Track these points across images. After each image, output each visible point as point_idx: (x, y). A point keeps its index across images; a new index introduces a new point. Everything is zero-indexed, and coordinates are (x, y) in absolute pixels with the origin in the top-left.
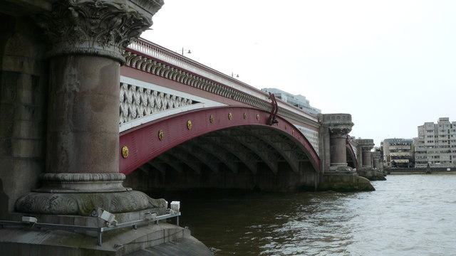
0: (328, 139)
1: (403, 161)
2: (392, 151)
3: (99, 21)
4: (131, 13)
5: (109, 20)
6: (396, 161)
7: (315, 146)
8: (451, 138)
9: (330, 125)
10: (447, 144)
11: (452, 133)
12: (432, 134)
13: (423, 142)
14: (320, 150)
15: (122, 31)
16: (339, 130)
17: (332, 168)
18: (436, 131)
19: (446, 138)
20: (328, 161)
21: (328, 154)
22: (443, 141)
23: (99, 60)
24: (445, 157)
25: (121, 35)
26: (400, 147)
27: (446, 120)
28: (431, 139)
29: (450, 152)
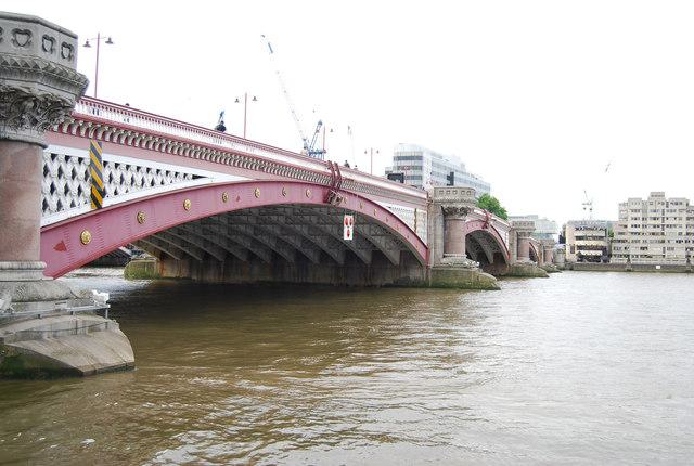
0: (440, 221)
1: (593, 253)
2: (579, 238)
3: (8, 105)
4: (44, 96)
5: (20, 103)
6: (583, 252)
7: (422, 232)
8: (666, 222)
9: (443, 202)
10: (659, 230)
11: (667, 215)
12: (639, 215)
13: (626, 227)
14: (429, 236)
15: (38, 114)
16: (455, 210)
17: (444, 260)
18: (645, 211)
19: (659, 222)
20: (440, 251)
21: (440, 241)
22: (655, 227)
23: (13, 145)
25: (37, 117)
26: (589, 233)
27: (661, 195)
28: (635, 222)
29: (663, 241)
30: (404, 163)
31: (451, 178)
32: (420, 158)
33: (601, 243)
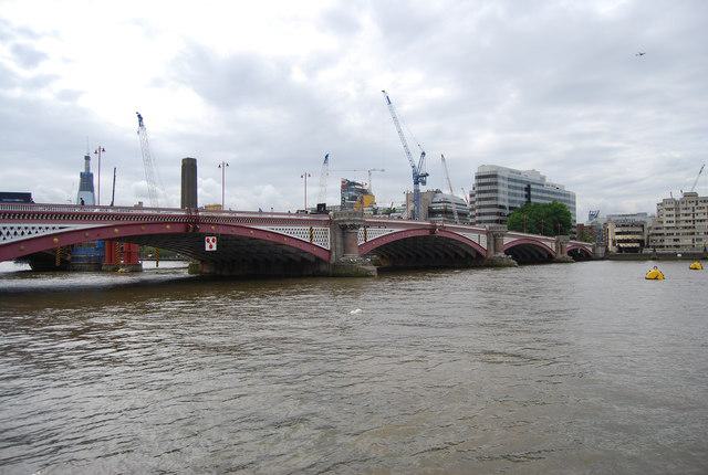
0: (339, 234)
2: (618, 233)
6: (621, 245)
8: (697, 218)
10: (691, 224)
11: (697, 211)
12: (673, 212)
18: (677, 209)
19: (690, 218)
24: (687, 241)
28: (670, 219)
29: (693, 234)
30: (483, 181)
31: (528, 189)
32: (495, 176)
33: (638, 237)
